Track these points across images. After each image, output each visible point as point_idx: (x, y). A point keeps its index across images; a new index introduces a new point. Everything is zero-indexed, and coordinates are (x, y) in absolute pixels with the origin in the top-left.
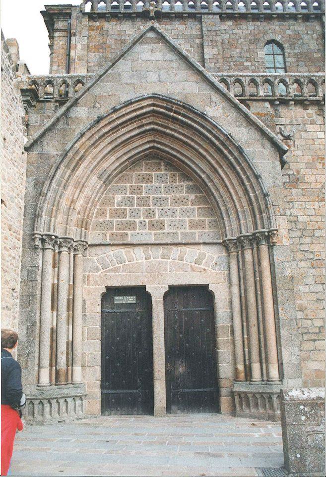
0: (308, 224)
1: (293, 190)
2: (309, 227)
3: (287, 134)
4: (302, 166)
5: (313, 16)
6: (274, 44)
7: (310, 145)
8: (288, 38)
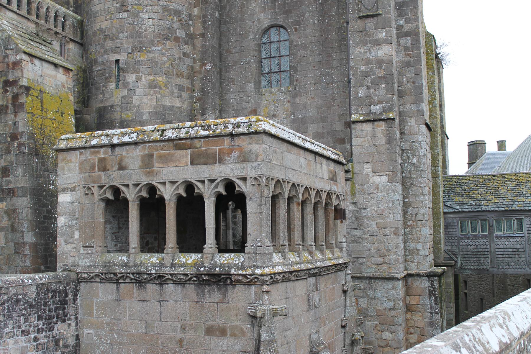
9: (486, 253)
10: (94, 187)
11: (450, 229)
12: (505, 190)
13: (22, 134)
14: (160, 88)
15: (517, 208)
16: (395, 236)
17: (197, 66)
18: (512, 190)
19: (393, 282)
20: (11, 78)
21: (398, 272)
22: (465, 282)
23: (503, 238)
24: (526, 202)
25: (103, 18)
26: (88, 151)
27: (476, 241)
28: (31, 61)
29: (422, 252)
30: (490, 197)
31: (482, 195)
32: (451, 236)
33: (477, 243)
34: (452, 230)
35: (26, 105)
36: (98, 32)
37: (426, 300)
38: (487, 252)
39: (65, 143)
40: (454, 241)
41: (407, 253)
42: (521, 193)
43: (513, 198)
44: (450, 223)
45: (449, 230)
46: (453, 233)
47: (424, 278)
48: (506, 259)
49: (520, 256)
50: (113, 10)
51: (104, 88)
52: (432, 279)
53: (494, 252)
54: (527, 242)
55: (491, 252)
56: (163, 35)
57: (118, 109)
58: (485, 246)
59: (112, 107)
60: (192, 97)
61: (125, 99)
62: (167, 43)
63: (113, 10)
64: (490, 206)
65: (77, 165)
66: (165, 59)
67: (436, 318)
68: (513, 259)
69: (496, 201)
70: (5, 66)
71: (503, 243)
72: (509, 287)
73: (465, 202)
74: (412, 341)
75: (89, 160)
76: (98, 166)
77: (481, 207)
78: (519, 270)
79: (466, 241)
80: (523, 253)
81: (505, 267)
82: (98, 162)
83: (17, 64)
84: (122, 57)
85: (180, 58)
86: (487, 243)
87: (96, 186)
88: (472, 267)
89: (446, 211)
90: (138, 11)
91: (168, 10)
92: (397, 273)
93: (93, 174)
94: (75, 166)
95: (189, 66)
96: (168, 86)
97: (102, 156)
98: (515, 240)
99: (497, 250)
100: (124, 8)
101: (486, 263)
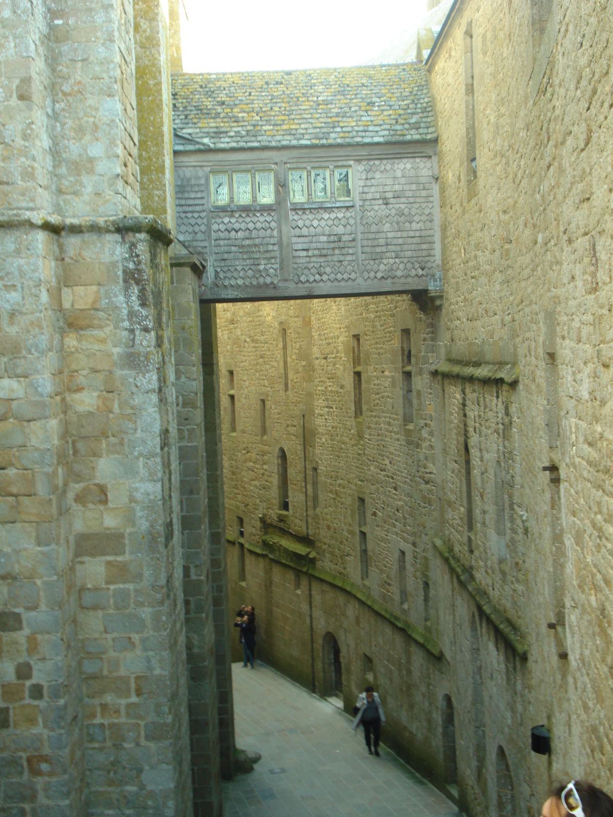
9: (271, 248)
11: (188, 192)
12: (311, 103)
15: (339, 141)
16: (19, 102)
18: (326, 103)
19: (18, 233)
21: (31, 205)
22: (231, 373)
23: (307, 212)
24: (356, 128)
27: (248, 220)
29: (100, 167)
30: (280, 118)
31: (260, 115)
32: (190, 209)
33: (251, 226)
34: (193, 195)
37: (116, 296)
38: (274, 244)
40: (199, 221)
41: (63, 170)
42: (347, 109)
43: (329, 120)
44: (189, 180)
45: (186, 195)
46: (197, 202)
47: (109, 237)
48: (314, 259)
49: (344, 251)
52: (130, 237)
53: (288, 245)
54: (358, 221)
55: (280, 243)
58: (269, 231)
64: (278, 138)
67: (145, 343)
68: (330, 258)
69: (293, 127)
71: (308, 223)
72: (317, 362)
73: (223, 130)
74: (81, 409)
77: (259, 138)
78: (343, 284)
79: (226, 220)
80: (350, 245)
81: (312, 279)
86: (273, 225)
88: (240, 282)
89: (180, 148)
92: (28, 209)
98: (333, 216)
99: (294, 240)
101: (272, 271)
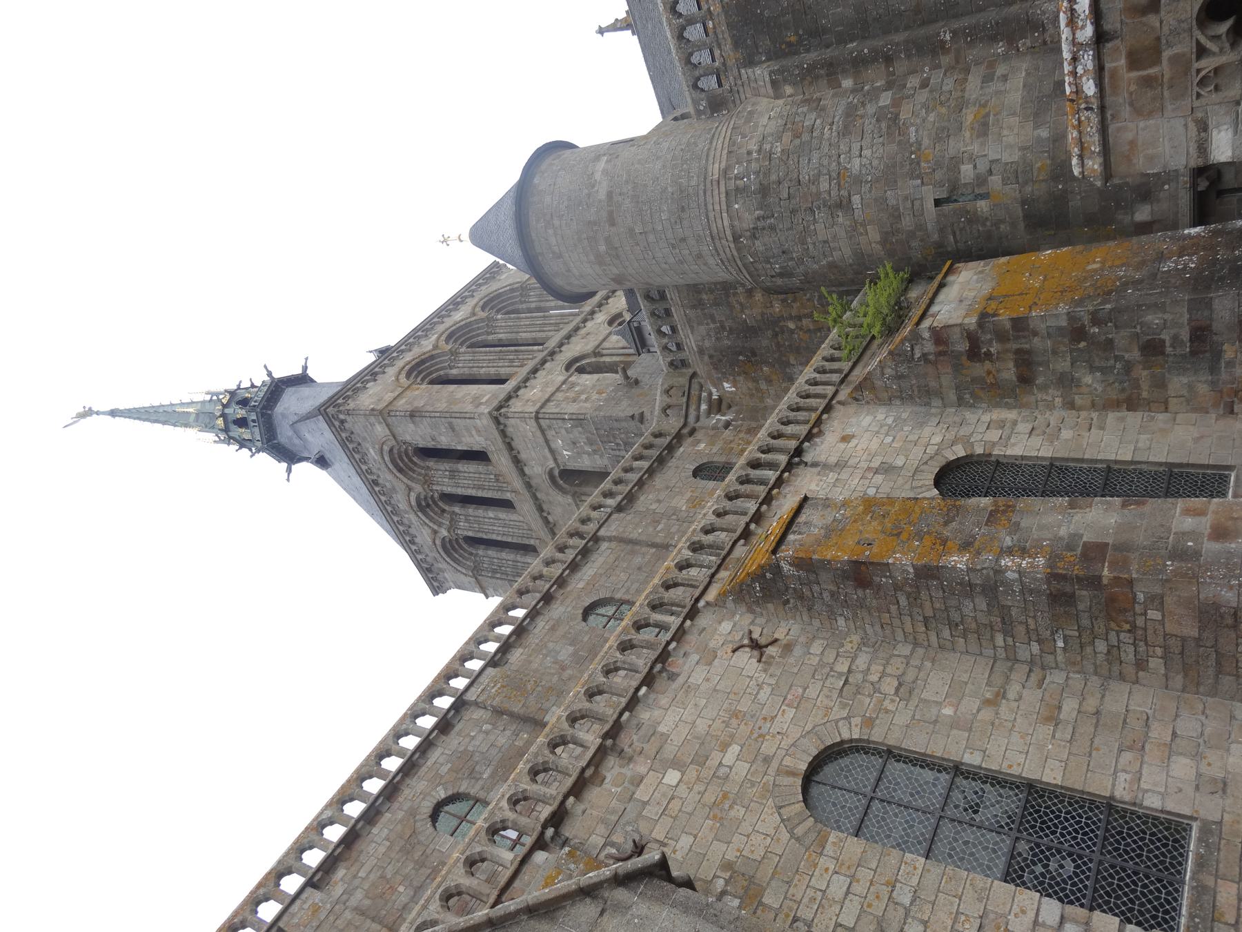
0: (870, 906)
1: (765, 900)
2: (878, 908)
3: (629, 847)
4: (719, 847)
5: (452, 712)
6: (446, 808)
7: (680, 810)
8: (455, 774)
10: (1198, 71)
13: (1071, 317)
14: (988, 115)
17: (946, 60)
20: (962, 346)
25: (862, 239)
26: (1109, 100)
28: (934, 316)
35: (1015, 316)
36: (888, 246)
39: (1089, 163)
50: (848, 223)
51: (988, 223)
56: (889, 127)
57: (1028, 189)
59: (1024, 202)
60: (1006, 57)
61: (1009, 178)
62: (902, 116)
63: (848, 223)
65: (1142, 124)
66: (932, 117)
70: (942, 358)
75: (1131, 94)
76: (1145, 69)
82: (1138, 69)
83: (939, 336)
84: (929, 195)
85: (931, 91)
87: (1196, 65)
90: (849, 177)
91: (846, 127)
93: (1166, 77)
94: (1143, 129)
95: (945, 74)
96: (983, 102)
97: (1123, 62)
100: (844, 202)
